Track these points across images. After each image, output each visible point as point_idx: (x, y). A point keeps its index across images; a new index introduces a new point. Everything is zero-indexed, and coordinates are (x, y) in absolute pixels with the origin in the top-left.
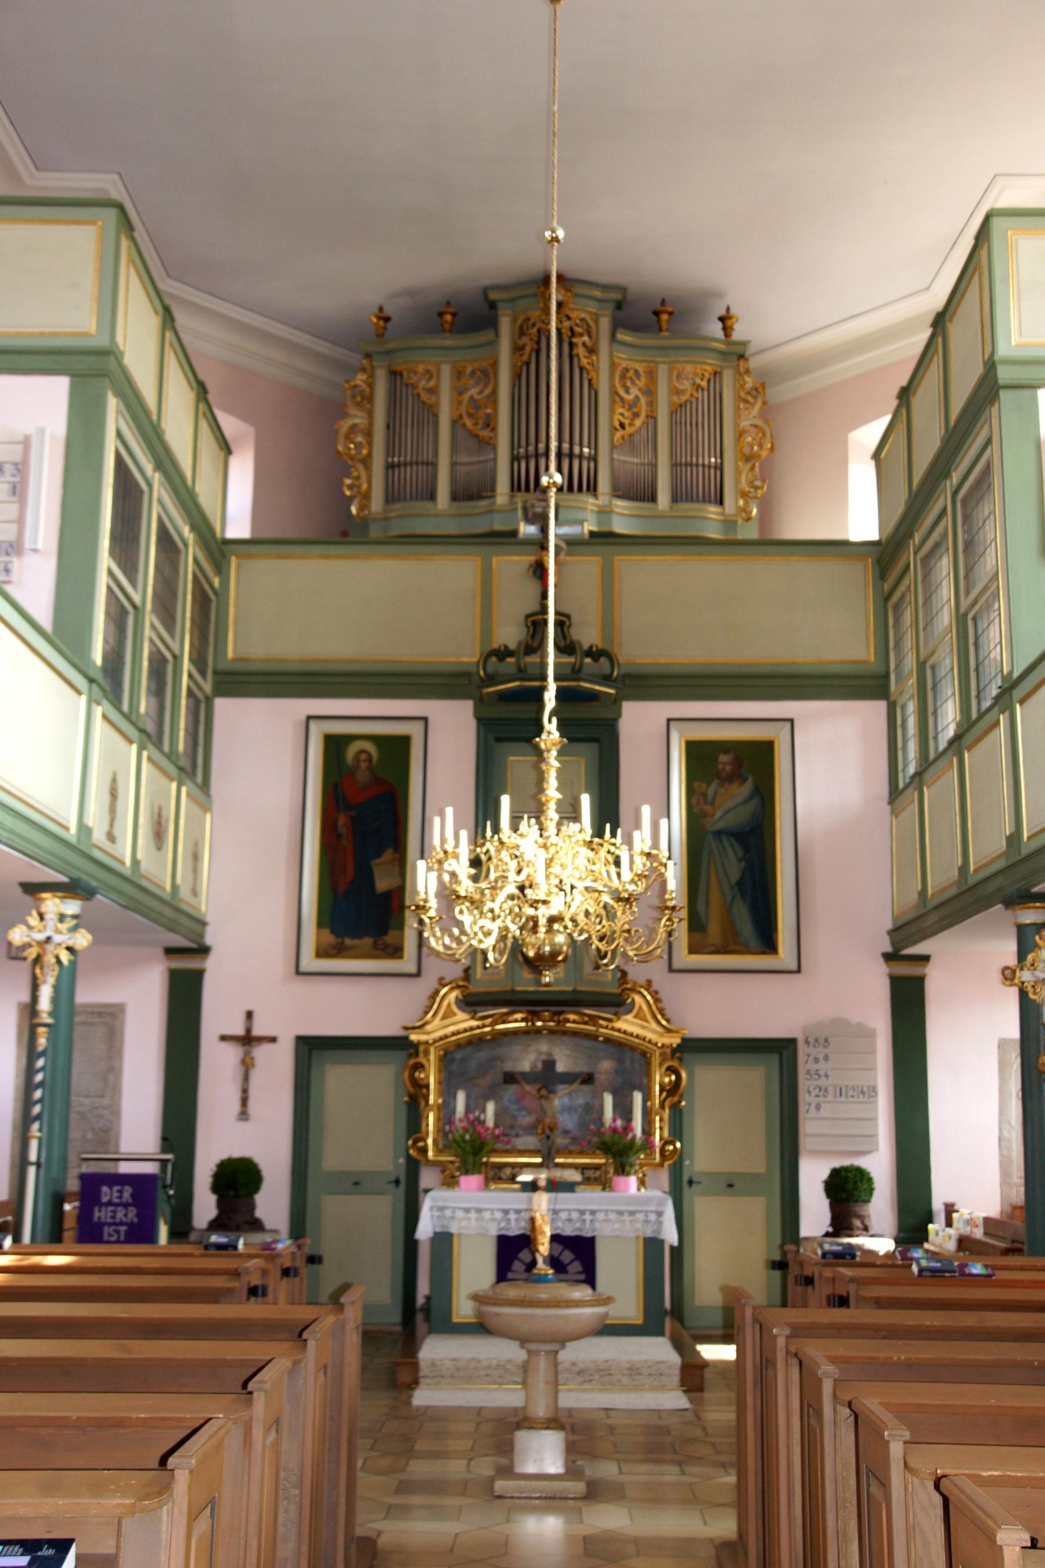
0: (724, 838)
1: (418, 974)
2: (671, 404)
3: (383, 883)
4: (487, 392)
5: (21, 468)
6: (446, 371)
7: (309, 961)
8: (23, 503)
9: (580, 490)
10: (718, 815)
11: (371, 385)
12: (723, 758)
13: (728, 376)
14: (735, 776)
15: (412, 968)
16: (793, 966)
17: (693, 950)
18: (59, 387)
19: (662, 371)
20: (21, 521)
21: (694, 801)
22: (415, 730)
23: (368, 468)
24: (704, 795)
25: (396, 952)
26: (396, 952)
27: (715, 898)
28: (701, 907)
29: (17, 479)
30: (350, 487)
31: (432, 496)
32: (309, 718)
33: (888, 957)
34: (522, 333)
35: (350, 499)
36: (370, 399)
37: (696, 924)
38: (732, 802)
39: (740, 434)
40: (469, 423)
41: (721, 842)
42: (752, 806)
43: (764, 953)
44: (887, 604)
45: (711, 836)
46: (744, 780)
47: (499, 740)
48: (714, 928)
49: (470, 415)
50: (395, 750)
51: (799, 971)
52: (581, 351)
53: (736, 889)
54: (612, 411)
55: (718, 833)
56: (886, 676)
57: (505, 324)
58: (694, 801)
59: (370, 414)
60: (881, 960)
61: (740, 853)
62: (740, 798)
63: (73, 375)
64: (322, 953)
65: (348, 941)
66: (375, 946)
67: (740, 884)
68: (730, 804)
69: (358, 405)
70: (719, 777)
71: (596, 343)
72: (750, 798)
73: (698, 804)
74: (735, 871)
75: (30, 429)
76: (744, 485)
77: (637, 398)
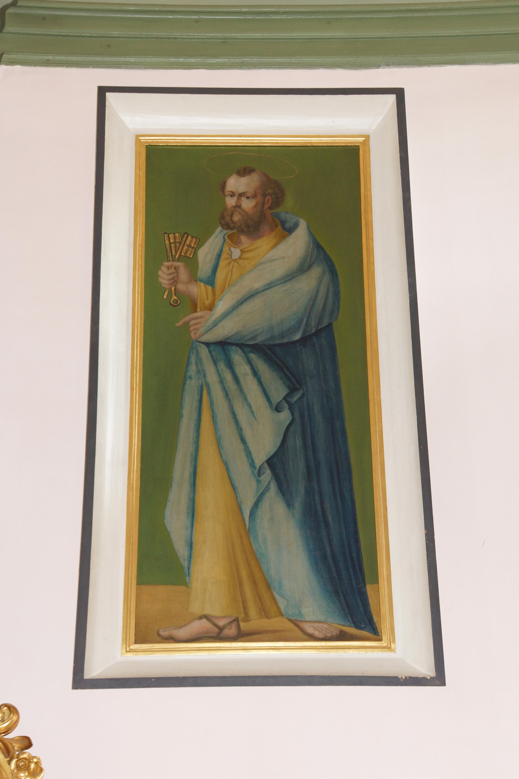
0: (237, 357)
10: (221, 307)
12: (234, 183)
14: (266, 220)
17: (145, 631)
21: (164, 277)
24: (191, 263)
27: (212, 495)
28: (175, 520)
37: (157, 560)
38: (259, 282)
41: (230, 365)
42: (307, 284)
43: (342, 636)
45: (204, 351)
46: (290, 231)
51: (439, 679)
53: (268, 474)
55: (224, 344)
58: (164, 277)
61: (279, 390)
62: (280, 270)
68: (252, 282)
70: (226, 226)
72: (303, 268)
73: (175, 281)
74: (265, 433)
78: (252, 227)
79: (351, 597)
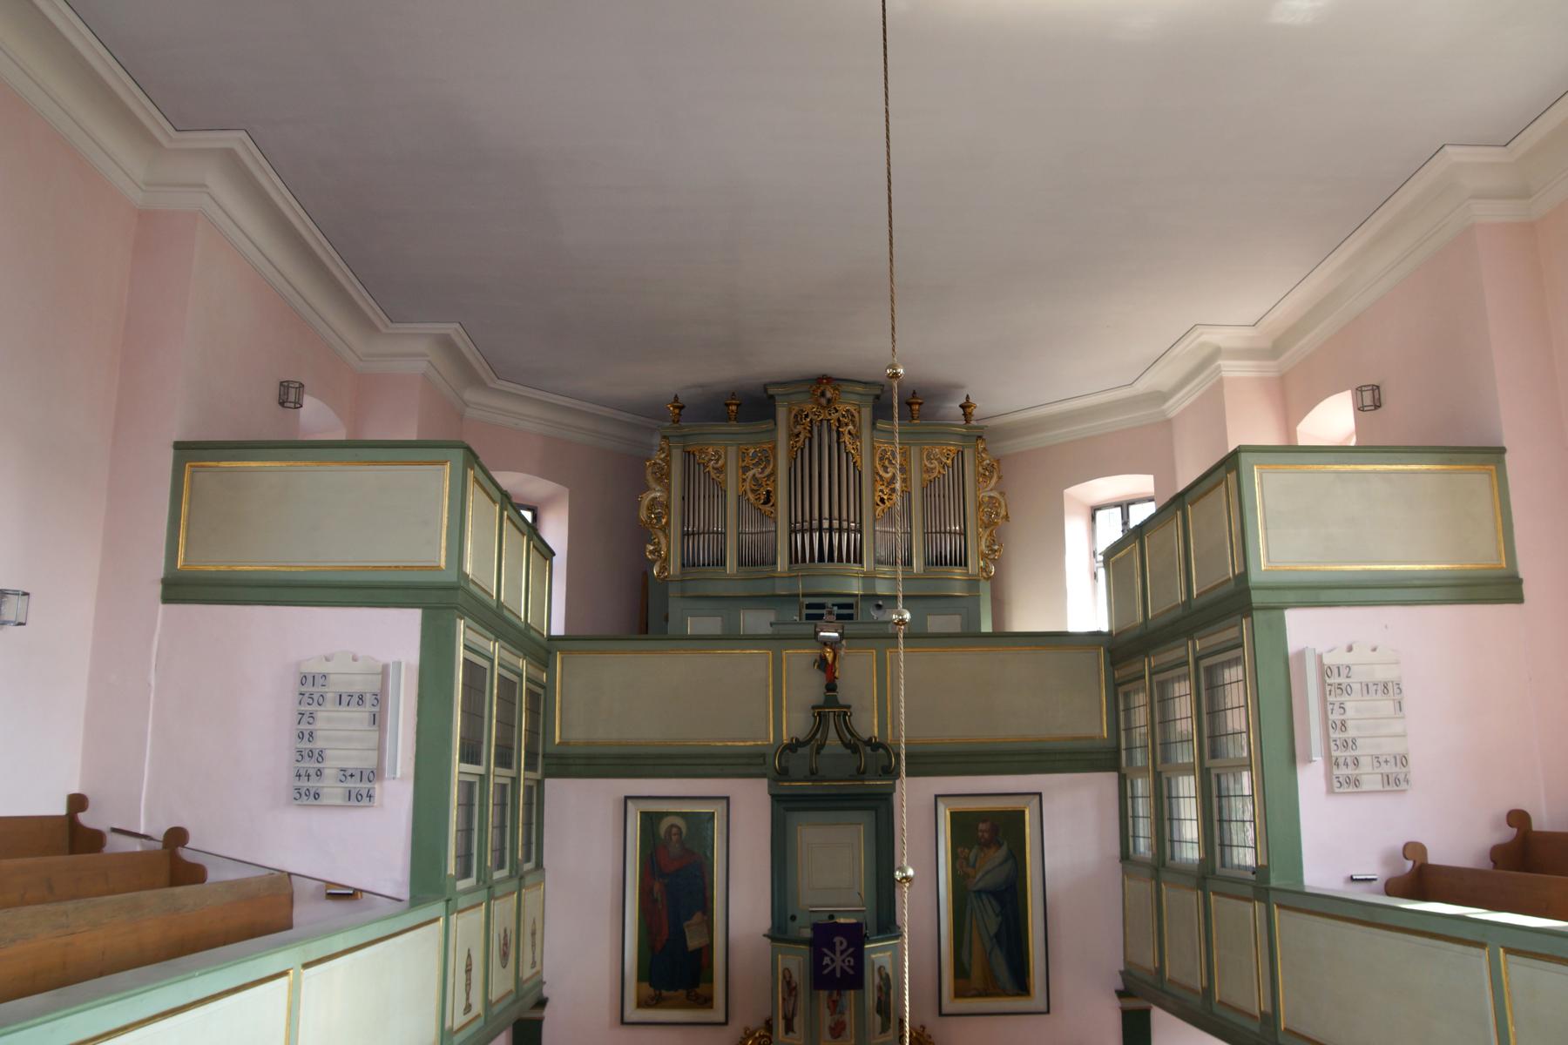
1: (726, 1023)
2: (922, 480)
3: (693, 943)
4: (767, 471)
5: (380, 698)
6: (732, 450)
7: (632, 1013)
8: (382, 730)
9: (848, 560)
11: (668, 463)
12: (982, 826)
13: (968, 454)
14: (993, 842)
15: (721, 1018)
16: (1043, 1007)
17: (959, 993)
18: (414, 616)
19: (914, 451)
20: (380, 749)
22: (717, 809)
23: (667, 537)
24: (967, 859)
25: (706, 1002)
26: (706, 1002)
29: (376, 709)
30: (652, 552)
31: (723, 564)
32: (627, 798)
33: (1121, 994)
34: (797, 422)
35: (653, 562)
36: (668, 476)
37: (960, 971)
38: (991, 862)
39: (980, 505)
40: (751, 496)
44: (1118, 691)
46: (1000, 845)
47: (788, 810)
48: (976, 972)
49: (753, 491)
50: (700, 824)
52: (847, 438)
54: (874, 490)
55: (979, 892)
56: (1118, 751)
57: (782, 413)
59: (668, 489)
60: (1115, 996)
63: (424, 608)
64: (642, 1004)
65: (665, 993)
66: (688, 996)
67: (997, 936)
69: (659, 480)
71: (859, 429)
72: (1005, 861)
74: (993, 924)
75: (389, 659)
76: (983, 547)
77: (894, 477)
78: (986, 845)
79: (1023, 988)
